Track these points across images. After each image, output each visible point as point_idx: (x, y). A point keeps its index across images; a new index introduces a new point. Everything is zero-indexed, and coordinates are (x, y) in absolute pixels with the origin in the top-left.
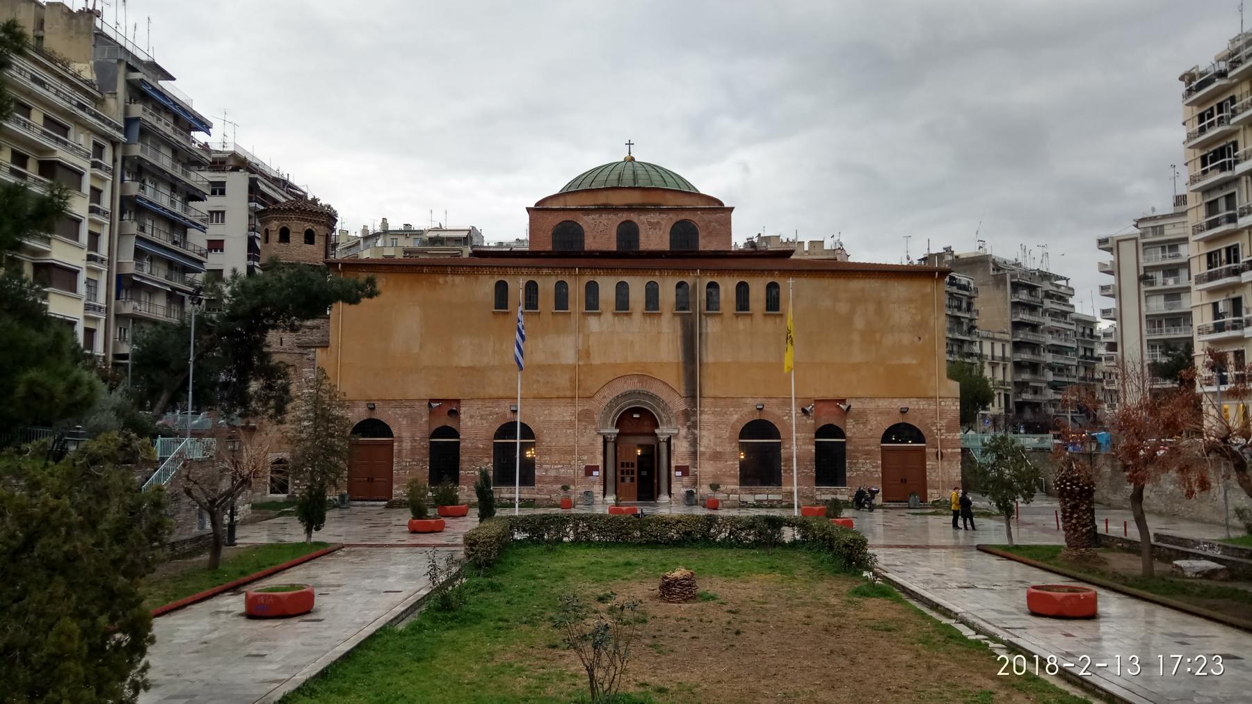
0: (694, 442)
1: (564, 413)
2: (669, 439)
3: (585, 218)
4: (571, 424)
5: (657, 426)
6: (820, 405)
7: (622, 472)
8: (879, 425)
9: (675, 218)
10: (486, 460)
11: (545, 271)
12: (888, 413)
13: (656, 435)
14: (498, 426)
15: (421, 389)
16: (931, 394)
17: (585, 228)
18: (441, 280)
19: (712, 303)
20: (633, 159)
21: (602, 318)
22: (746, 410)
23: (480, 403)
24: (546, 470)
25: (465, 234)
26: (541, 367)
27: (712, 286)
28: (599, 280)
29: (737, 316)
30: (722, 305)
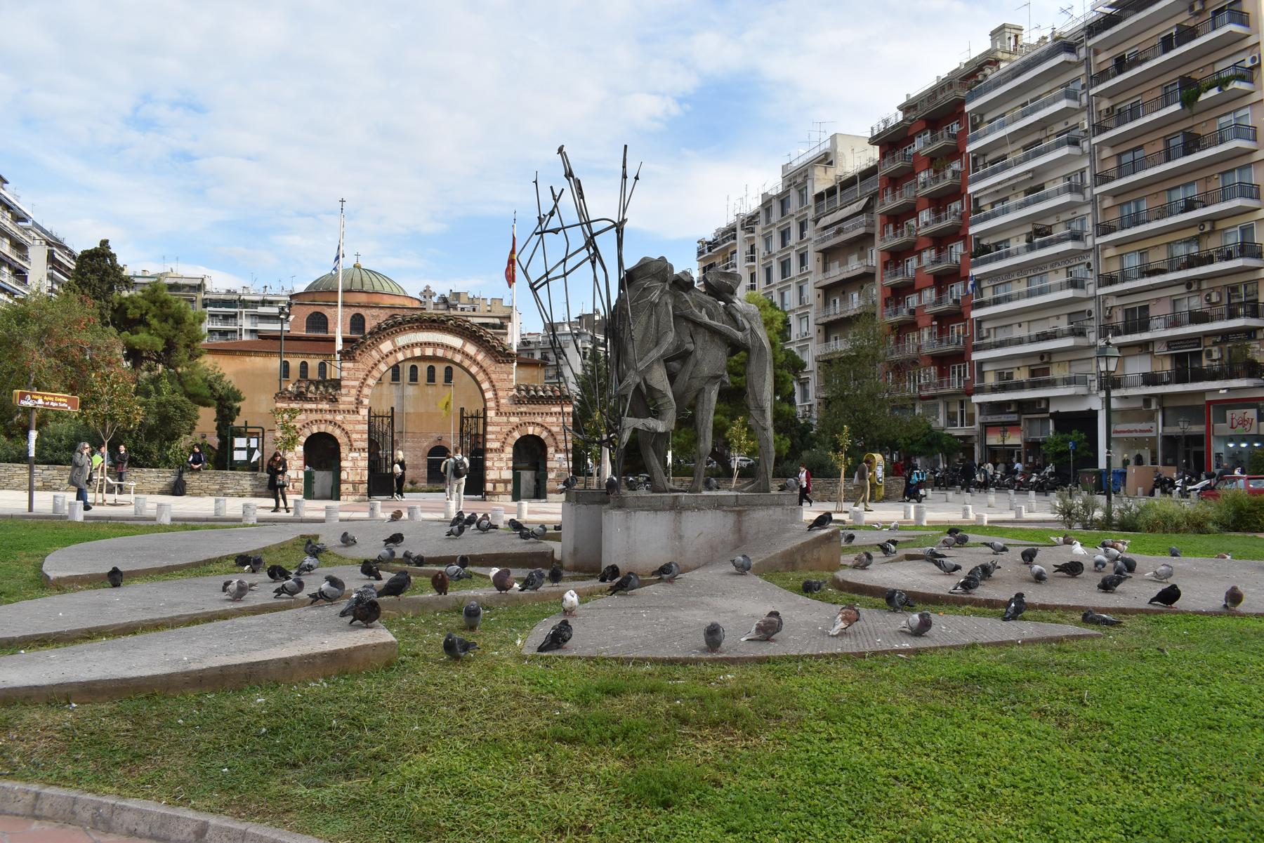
9: (390, 312)
19: (414, 378)
20: (359, 268)
25: (199, 282)
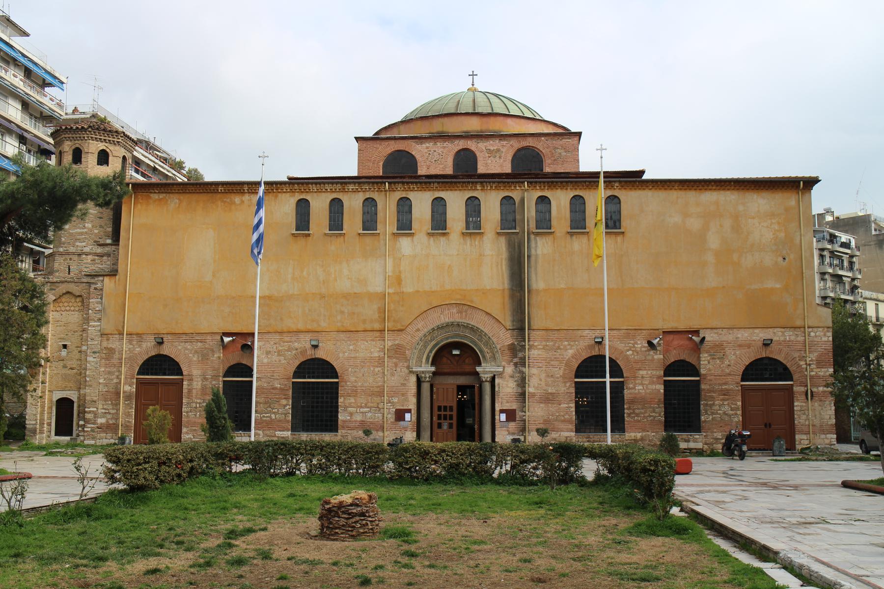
0: (522, 382)
1: (369, 348)
2: (493, 378)
3: (419, 147)
4: (381, 362)
5: (480, 364)
6: (670, 337)
7: (439, 417)
8: (738, 360)
9: (516, 144)
10: (284, 402)
11: (351, 187)
12: (749, 346)
13: (477, 374)
14: (297, 363)
15: (215, 321)
16: (799, 323)
17: (418, 157)
18: (237, 199)
19: (544, 223)
21: (416, 238)
22: (583, 344)
23: (277, 336)
24: (351, 414)
26: (346, 296)
27: (543, 200)
28: (412, 195)
29: (571, 234)
30: (554, 223)
